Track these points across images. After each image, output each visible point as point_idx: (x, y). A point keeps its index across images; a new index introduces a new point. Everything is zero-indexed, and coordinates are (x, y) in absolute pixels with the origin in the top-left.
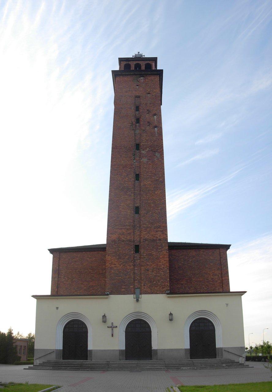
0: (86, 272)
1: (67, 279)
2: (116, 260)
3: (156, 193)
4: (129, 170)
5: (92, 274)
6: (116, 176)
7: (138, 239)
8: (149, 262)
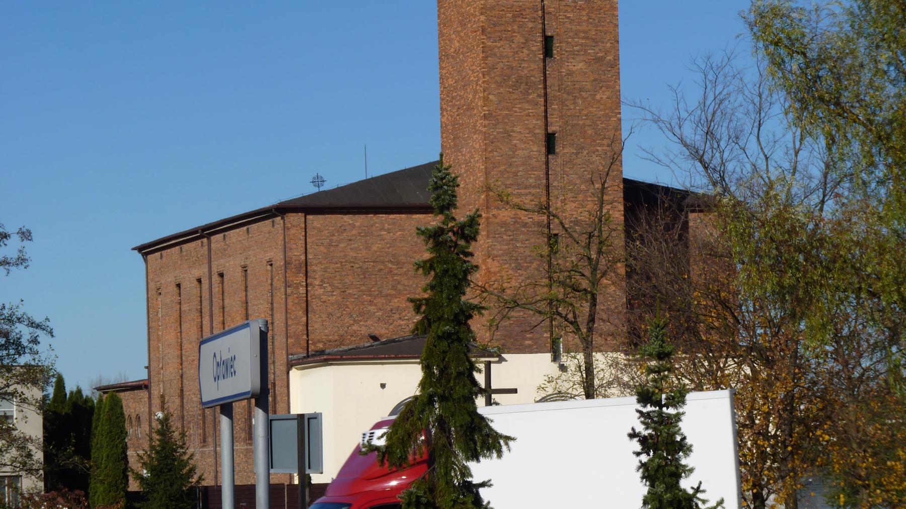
0: (380, 270)
1: (329, 289)
3: (598, 97)
4: (530, 25)
6: (499, 45)
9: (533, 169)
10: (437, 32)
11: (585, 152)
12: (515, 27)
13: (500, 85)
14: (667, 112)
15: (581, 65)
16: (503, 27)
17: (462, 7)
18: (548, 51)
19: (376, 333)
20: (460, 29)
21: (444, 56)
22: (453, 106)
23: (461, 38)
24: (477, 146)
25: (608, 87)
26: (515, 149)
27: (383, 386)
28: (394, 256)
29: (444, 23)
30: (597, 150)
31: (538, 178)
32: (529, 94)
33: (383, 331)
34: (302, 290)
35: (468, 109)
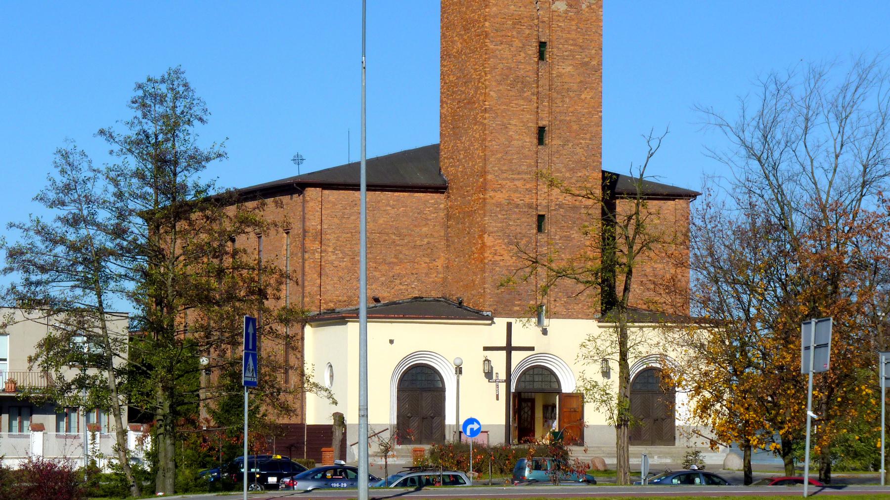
0: (385, 240)
1: (341, 255)
2: (504, 246)
3: (583, 97)
4: (527, 32)
5: (398, 245)
6: (500, 48)
7: (544, 203)
8: (564, 253)
9: (526, 157)
10: (440, 34)
11: (570, 145)
12: (515, 33)
13: (499, 83)
14: (732, 117)
15: (570, 68)
16: (504, 33)
17: (465, 13)
18: (541, 56)
19: (378, 295)
20: (463, 32)
21: (445, 55)
22: (453, 100)
23: (465, 40)
24: (477, 136)
25: (592, 89)
26: (511, 139)
27: (391, 342)
28: (397, 228)
29: (446, 26)
30: (581, 143)
31: (529, 166)
32: (525, 92)
33: (386, 294)
34: (317, 256)
35: (469, 103)
